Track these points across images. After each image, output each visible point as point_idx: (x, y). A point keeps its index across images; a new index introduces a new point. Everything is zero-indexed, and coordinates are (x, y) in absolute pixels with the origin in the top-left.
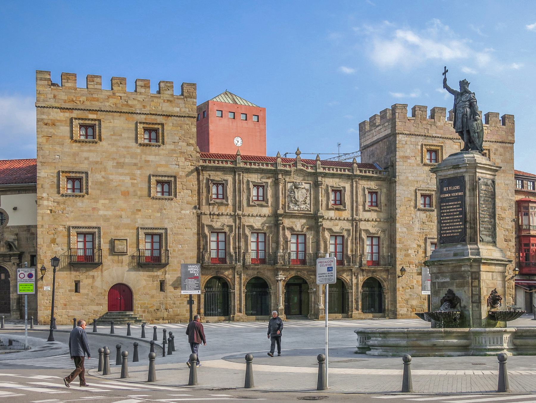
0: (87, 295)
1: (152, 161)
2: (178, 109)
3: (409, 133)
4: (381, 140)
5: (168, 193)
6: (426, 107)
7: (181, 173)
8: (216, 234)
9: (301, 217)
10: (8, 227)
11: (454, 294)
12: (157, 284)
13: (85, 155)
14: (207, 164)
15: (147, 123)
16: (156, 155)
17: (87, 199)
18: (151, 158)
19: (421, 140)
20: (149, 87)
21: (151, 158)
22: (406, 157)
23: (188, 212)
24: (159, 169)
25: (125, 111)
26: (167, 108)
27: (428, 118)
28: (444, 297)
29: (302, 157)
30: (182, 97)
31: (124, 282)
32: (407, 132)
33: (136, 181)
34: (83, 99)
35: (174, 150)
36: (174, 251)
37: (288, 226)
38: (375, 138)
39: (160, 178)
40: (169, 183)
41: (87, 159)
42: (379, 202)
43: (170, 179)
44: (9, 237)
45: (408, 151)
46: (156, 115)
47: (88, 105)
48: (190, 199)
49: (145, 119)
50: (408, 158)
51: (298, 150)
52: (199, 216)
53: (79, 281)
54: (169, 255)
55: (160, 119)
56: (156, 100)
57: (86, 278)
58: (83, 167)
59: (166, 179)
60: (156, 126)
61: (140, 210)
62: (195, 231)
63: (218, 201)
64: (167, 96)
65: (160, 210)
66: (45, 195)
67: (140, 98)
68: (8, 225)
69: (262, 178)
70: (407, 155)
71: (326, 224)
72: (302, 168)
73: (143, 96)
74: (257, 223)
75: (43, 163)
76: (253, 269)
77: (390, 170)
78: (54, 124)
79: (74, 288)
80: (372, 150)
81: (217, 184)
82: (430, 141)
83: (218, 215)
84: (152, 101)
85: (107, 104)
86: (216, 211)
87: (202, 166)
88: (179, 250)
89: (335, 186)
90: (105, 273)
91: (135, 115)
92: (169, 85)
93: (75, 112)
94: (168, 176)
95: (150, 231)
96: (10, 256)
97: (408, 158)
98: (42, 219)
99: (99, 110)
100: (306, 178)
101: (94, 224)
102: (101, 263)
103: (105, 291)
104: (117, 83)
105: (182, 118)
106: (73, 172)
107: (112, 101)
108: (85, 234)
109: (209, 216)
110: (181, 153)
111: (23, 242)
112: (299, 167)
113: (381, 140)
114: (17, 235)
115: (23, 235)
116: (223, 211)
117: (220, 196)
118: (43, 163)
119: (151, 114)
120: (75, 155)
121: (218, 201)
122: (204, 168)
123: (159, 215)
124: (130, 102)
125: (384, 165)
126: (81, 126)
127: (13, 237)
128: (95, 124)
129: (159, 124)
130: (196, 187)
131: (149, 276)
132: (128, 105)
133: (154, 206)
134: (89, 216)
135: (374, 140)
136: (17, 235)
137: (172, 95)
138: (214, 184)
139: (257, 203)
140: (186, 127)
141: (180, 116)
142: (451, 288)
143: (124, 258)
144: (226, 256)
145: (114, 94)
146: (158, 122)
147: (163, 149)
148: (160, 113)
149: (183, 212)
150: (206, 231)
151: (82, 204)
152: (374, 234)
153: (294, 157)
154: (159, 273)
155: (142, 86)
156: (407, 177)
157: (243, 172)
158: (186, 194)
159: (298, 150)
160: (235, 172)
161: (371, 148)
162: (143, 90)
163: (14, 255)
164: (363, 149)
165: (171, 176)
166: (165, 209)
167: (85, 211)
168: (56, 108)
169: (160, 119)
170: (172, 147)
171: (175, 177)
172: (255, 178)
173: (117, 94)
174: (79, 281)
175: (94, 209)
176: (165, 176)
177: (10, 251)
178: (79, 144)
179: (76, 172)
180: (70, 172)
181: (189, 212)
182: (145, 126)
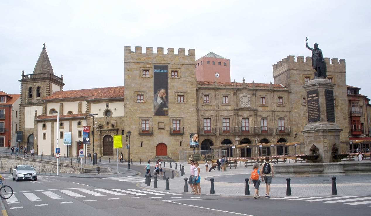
0: (147, 148)
1: (175, 86)
2: (186, 62)
4: (283, 73)
5: (183, 101)
6: (303, 57)
7: (189, 91)
8: (206, 119)
9: (247, 110)
10: (112, 117)
11: (316, 147)
12: (179, 143)
13: (145, 84)
14: (200, 87)
15: (172, 68)
16: (177, 83)
17: (146, 104)
18: (175, 84)
19: (303, 73)
20: (174, 51)
21: (175, 84)
22: (295, 80)
23: (192, 109)
24: (179, 90)
25: (163, 63)
26: (182, 61)
27: (304, 62)
28: (311, 148)
29: (246, 82)
30: (189, 55)
31: (163, 142)
32: (296, 69)
34: (145, 58)
35: (185, 81)
36: (186, 127)
37: (240, 115)
38: (280, 72)
39: (179, 94)
40: (183, 96)
41: (146, 85)
42: (283, 103)
43: (184, 94)
44: (113, 122)
45: (296, 78)
46: (177, 64)
47: (147, 61)
48: (193, 103)
49: (172, 66)
50: (297, 81)
51: (244, 78)
52: (198, 111)
53: (143, 142)
54: (184, 129)
55: (179, 66)
56: (177, 57)
57: (146, 140)
58: (144, 89)
59: (182, 94)
60: (177, 70)
63: (206, 104)
64: (182, 55)
65: (180, 109)
66: (128, 103)
67: (170, 56)
68: (112, 116)
69: (227, 92)
71: (259, 114)
72: (246, 87)
73: (171, 56)
74: (226, 114)
75: (127, 88)
76: (224, 135)
77: (288, 87)
78: (131, 70)
79: (140, 145)
80: (279, 78)
81: (206, 96)
82: (306, 73)
83: (206, 110)
84: (175, 58)
85: (155, 60)
86: (205, 108)
87: (198, 88)
88: (189, 127)
89: (263, 95)
90: (155, 138)
92: (182, 50)
93: (141, 64)
94: (183, 93)
95: (174, 119)
96: (113, 130)
97: (297, 81)
98: (127, 113)
99: (151, 63)
100: (248, 92)
101: (149, 116)
102: (153, 134)
103: (155, 146)
104: (160, 50)
105: (189, 66)
106: (140, 92)
107: (158, 58)
108: (145, 120)
109: (202, 111)
110: (189, 82)
111: (119, 124)
112: (244, 87)
113: (283, 73)
114: (116, 121)
115: (119, 121)
116: (209, 109)
117: (208, 102)
118: (127, 88)
119: (174, 64)
120: (141, 84)
121: (206, 104)
122: (200, 88)
123: (179, 111)
124: (165, 59)
125: (285, 85)
126: (143, 70)
127: (115, 122)
128: (149, 69)
129: (178, 68)
130: (195, 97)
131: (175, 140)
132: (164, 60)
133: (177, 107)
134: (147, 112)
135: (280, 73)
136: (116, 121)
137: (184, 55)
138: (204, 96)
139: (225, 104)
140: (190, 69)
141: (188, 65)
142: (314, 144)
143: (163, 131)
144: (211, 130)
145: (158, 55)
146: (178, 68)
147: (180, 80)
148: (179, 63)
149: (190, 109)
150: (201, 118)
152: (282, 117)
153: (242, 82)
155: (170, 51)
156: (296, 90)
157: (218, 90)
158: (192, 101)
159: (244, 78)
160: (214, 90)
161: (279, 77)
162: (171, 53)
163: (115, 130)
164: (275, 77)
165: (184, 93)
166: (182, 108)
167: (145, 110)
168: (132, 62)
170: (185, 79)
171: (186, 93)
172: (225, 93)
173: (159, 55)
174: (143, 142)
175: (149, 108)
176: (181, 93)
177: (113, 128)
178: (143, 79)
179: (141, 92)
180: (138, 92)
181: (193, 109)
182: (172, 69)
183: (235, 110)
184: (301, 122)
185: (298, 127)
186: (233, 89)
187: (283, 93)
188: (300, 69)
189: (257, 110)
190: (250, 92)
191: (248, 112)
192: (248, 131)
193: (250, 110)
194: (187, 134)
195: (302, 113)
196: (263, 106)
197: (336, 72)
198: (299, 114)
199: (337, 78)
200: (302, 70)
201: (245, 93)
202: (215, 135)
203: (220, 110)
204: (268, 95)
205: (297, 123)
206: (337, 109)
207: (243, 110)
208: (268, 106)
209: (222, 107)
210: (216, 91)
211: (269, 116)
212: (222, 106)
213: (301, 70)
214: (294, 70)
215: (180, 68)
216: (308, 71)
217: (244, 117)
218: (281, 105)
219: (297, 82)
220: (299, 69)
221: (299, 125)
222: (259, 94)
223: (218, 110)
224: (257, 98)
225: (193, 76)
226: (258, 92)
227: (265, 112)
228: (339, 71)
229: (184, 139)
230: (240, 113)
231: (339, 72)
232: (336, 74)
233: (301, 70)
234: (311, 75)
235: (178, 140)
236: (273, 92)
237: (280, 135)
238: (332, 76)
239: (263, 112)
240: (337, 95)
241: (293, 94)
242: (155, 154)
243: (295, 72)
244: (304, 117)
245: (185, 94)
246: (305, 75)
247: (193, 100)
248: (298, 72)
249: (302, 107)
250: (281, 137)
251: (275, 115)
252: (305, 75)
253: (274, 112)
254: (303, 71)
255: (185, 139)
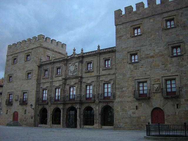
3: (121, 23)
7: (34, 69)
9: (73, 78)
12: (24, 111)
23: (34, 83)
32: (120, 23)
33: (22, 74)
39: (28, 72)
45: (122, 33)
51: (74, 48)
55: (30, 51)
61: (22, 84)
62: (35, 90)
70: (121, 35)
71: (84, 80)
82: (135, 23)
91: (25, 52)
97: (122, 36)
149: (33, 83)
151: (10, 84)
154: (24, 107)
157: (54, 64)
159: (74, 48)
169: (30, 51)
183: (63, 79)
184: (126, 85)
185: (122, 92)
186: (63, 60)
187: (110, 54)
188: (127, 21)
189: (81, 77)
190: (78, 60)
191: (74, 80)
192: (74, 99)
193: (77, 77)
194: (29, 104)
195: (129, 73)
196: (89, 72)
197: (178, 9)
198: (124, 75)
199: (181, 16)
200: (129, 22)
201: (74, 60)
202: (48, 104)
203: (54, 81)
204: (95, 60)
205: (121, 86)
206: (183, 59)
207: (69, 78)
208: (93, 72)
209: (55, 78)
210: (52, 65)
211: (93, 81)
212: (55, 77)
213: (128, 22)
214: (120, 24)
215: (30, 52)
216: (137, 20)
217: (71, 85)
218: (107, 68)
219: (123, 38)
220: (125, 22)
221: (124, 89)
222: (86, 60)
223: (52, 81)
224: (83, 64)
225: (38, 56)
226: (85, 58)
227: (90, 78)
228: (185, 6)
229: (27, 108)
230: (68, 82)
231: (184, 8)
232: (180, 12)
233: (128, 22)
234: (141, 24)
235: (24, 108)
236: (100, 55)
237: (104, 102)
238: (172, 16)
239: (89, 78)
240: (182, 40)
241: (118, 52)
242: (11, 120)
243: (121, 26)
244: (130, 79)
245: (31, 71)
246: (133, 27)
247: (35, 75)
248: (124, 26)
249: (128, 66)
250: (105, 105)
251: (100, 80)
252: (133, 27)
253: (99, 76)
254: (131, 22)
255: (29, 108)
